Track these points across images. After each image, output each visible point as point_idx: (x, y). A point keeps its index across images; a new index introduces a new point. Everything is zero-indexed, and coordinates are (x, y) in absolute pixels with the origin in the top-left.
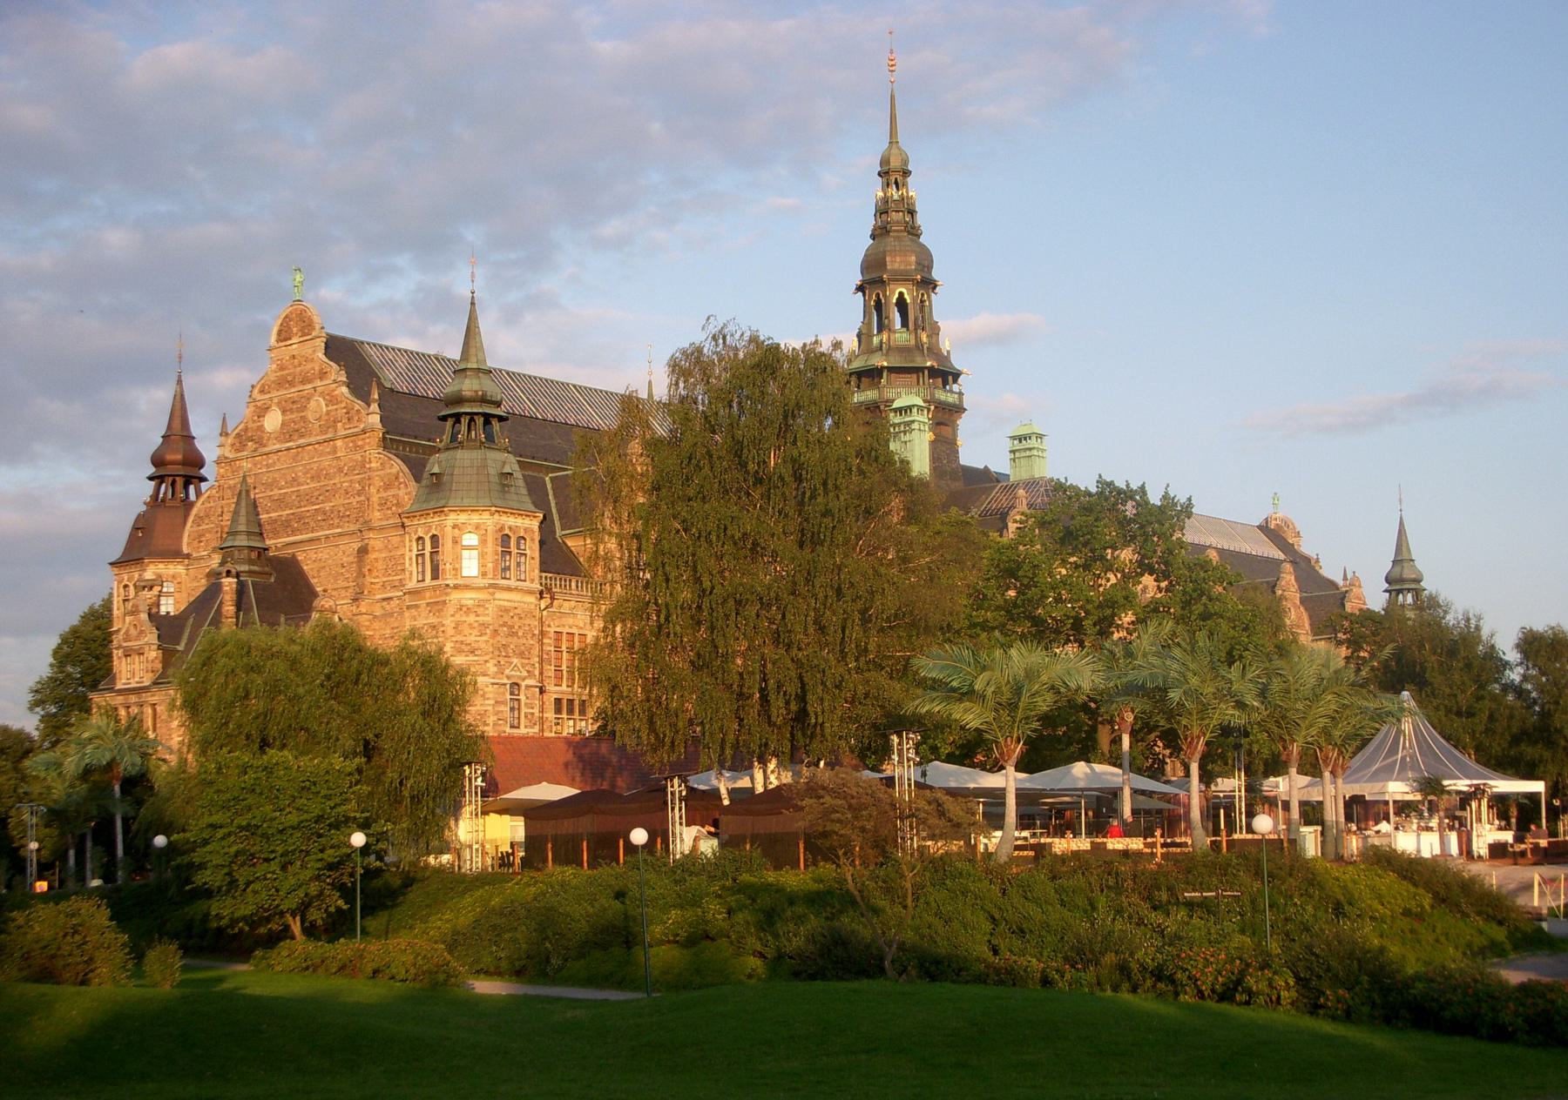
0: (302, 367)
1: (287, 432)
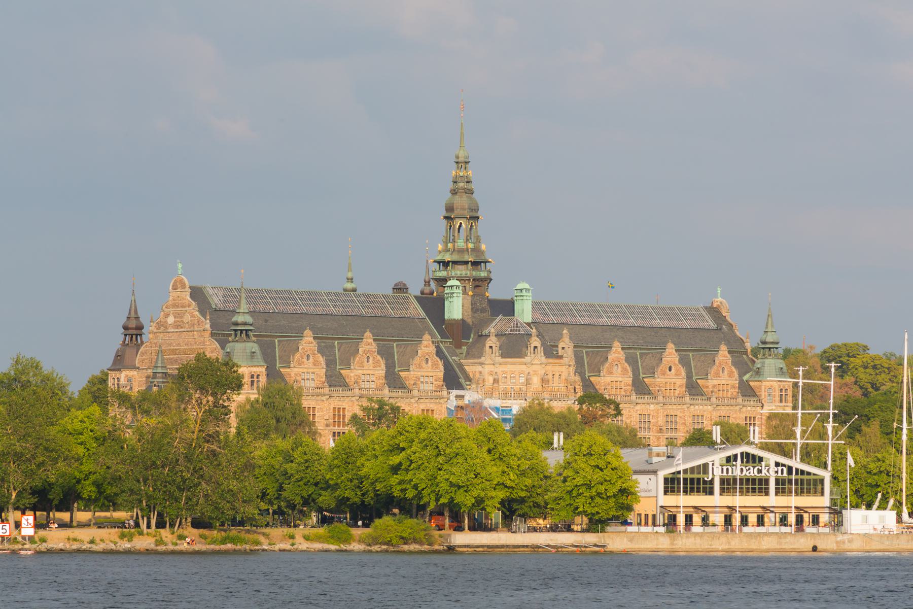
1: (177, 325)
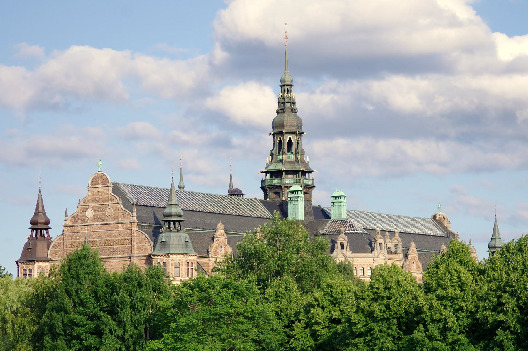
0: (103, 196)
1: (96, 218)
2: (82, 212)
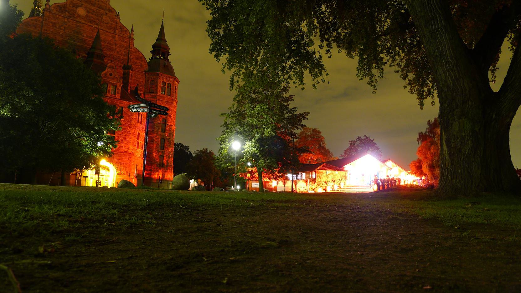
2: (71, 6)
